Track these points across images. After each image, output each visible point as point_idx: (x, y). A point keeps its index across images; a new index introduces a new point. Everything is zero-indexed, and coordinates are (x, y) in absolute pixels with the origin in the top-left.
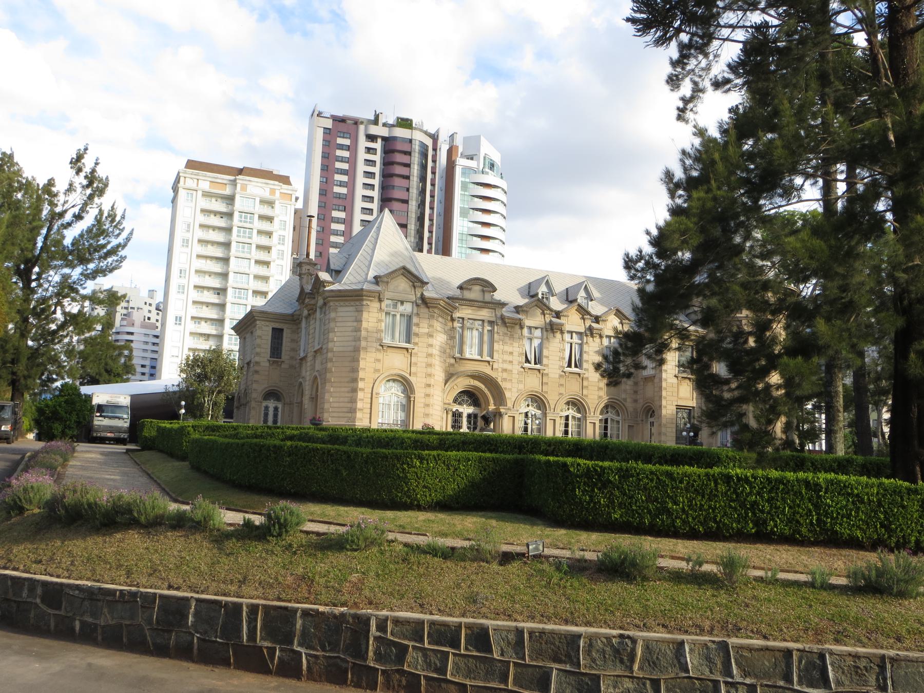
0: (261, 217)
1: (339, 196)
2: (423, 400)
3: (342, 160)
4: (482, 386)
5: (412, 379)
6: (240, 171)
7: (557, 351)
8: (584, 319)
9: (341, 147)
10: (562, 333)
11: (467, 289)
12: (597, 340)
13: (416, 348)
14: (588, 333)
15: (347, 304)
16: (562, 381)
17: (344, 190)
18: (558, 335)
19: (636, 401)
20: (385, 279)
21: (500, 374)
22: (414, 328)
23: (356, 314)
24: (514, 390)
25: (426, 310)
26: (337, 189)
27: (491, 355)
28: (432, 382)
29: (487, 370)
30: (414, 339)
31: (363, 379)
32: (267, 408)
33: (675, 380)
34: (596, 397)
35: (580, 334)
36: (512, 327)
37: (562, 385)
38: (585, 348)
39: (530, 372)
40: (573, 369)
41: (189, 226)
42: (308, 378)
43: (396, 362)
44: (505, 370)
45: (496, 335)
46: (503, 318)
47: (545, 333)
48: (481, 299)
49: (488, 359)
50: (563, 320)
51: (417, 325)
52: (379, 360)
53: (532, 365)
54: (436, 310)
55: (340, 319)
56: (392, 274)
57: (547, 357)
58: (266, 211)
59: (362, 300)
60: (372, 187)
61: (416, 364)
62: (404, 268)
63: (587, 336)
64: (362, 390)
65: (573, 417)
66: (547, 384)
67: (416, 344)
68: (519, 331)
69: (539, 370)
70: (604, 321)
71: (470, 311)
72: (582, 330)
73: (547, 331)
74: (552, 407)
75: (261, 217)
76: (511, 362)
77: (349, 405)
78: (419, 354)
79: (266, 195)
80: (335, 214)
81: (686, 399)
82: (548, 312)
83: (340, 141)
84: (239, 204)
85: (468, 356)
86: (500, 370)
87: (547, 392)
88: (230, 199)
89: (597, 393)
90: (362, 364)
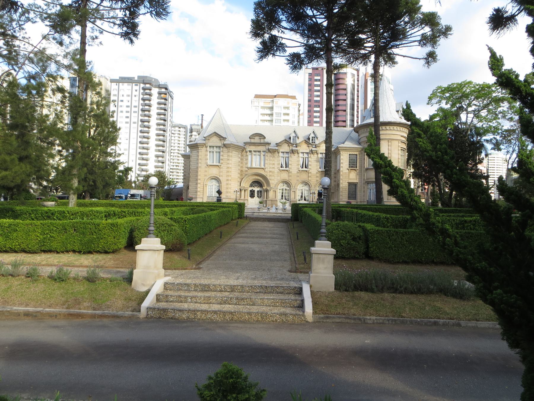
0: (285, 114)
1: (316, 101)
3: (317, 86)
4: (261, 179)
6: (275, 96)
7: (296, 161)
9: (316, 80)
10: (298, 153)
12: (316, 155)
16: (299, 175)
17: (318, 99)
18: (296, 155)
22: (221, 157)
26: (316, 99)
27: (265, 166)
29: (262, 172)
30: (221, 161)
31: (200, 179)
35: (307, 153)
38: (310, 159)
40: (304, 169)
43: (214, 172)
44: (270, 172)
46: (269, 149)
48: (259, 142)
49: (263, 167)
50: (298, 148)
51: (222, 155)
52: (206, 171)
53: (285, 169)
56: (210, 136)
58: (286, 111)
62: (215, 133)
64: (200, 183)
65: (286, 189)
67: (222, 163)
72: (308, 151)
75: (285, 114)
79: (286, 105)
80: (315, 109)
81: (353, 179)
83: (316, 78)
84: (275, 110)
85: (254, 166)
88: (272, 108)
90: (199, 173)
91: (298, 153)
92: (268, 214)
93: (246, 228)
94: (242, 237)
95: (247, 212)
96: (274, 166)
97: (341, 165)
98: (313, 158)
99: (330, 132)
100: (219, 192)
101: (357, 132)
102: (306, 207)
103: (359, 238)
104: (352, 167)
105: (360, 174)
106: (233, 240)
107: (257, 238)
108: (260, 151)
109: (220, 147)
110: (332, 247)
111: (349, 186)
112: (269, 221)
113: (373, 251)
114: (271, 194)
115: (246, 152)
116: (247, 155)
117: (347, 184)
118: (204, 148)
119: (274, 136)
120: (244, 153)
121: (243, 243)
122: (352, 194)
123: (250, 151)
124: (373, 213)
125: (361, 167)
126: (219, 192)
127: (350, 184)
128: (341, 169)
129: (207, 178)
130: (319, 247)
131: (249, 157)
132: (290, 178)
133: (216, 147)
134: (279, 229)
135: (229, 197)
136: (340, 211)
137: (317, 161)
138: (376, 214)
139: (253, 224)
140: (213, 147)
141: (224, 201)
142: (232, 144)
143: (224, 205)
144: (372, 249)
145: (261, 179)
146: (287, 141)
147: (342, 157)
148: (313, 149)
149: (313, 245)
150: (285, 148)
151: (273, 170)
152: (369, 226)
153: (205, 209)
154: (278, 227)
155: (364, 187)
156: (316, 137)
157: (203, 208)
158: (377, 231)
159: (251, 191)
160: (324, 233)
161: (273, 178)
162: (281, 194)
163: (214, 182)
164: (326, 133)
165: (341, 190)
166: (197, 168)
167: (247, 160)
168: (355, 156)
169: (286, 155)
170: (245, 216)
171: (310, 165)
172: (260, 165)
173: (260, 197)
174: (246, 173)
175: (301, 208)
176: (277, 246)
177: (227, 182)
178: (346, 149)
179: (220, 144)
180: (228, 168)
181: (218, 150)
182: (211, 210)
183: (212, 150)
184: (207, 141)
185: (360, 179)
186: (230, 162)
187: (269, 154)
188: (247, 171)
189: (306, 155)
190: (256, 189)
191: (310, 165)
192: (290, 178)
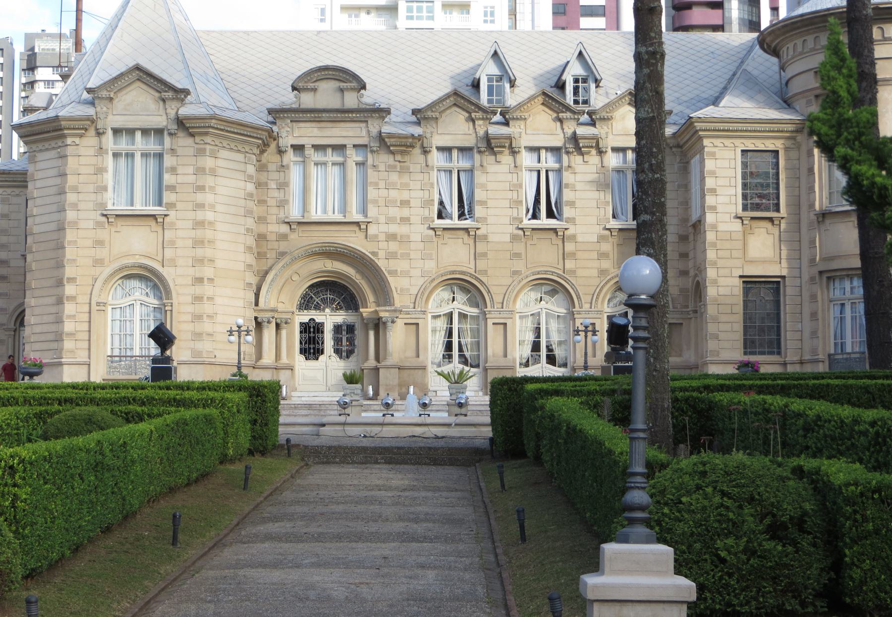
2: (190, 309)
4: (349, 271)
5: (166, 272)
7: (501, 190)
8: (561, 121)
10: (514, 152)
11: (306, 90)
13: (172, 213)
14: (570, 146)
15: (47, 146)
16: (519, 247)
20: (104, 93)
21: (383, 245)
22: (168, 178)
23: (59, 162)
24: (416, 273)
25: (189, 141)
27: (364, 212)
29: (354, 241)
30: (168, 197)
31: (72, 280)
33: (737, 226)
34: (595, 273)
35: (555, 150)
36: (402, 153)
37: (517, 255)
38: (567, 177)
39: (447, 235)
40: (544, 221)
41: (323, 11)
43: (137, 244)
44: (391, 237)
45: (370, 171)
46: (381, 138)
47: (477, 157)
49: (358, 217)
50: (513, 130)
51: (173, 170)
52: (99, 243)
53: (455, 222)
54: (208, 139)
55: (39, 175)
56: (117, 83)
57: (483, 203)
59: (64, 136)
61: (172, 242)
62: (138, 68)
63: (568, 153)
64: (72, 298)
66: (485, 255)
68: (421, 158)
69: (466, 230)
70: (603, 119)
71: (316, 132)
72: (558, 142)
73: (480, 152)
74: (498, 299)
76: (405, 220)
77: (53, 328)
78: (179, 224)
81: (764, 261)
82: (480, 114)
85: (316, 214)
86: (382, 237)
87: (485, 272)
89: (596, 264)
90: (70, 252)
91: (514, 152)
92: (388, 432)
93: (288, 495)
94: (269, 537)
95: (290, 423)
96: (405, 212)
97: (710, 200)
98: (583, 171)
99: (653, 54)
100: (162, 337)
101: (775, 53)
102: (558, 393)
103: (800, 522)
104: (757, 207)
105: (794, 239)
106: (228, 554)
107: (339, 538)
108: (339, 148)
109: (159, 132)
110: (678, 572)
111: (746, 292)
112: (389, 462)
113: (863, 582)
114: (397, 338)
115: (281, 152)
116: (283, 168)
117: (738, 282)
118: (90, 140)
119: (401, 81)
120: (270, 155)
121: (275, 565)
122: (762, 330)
123: (299, 148)
124: (857, 411)
125: (796, 205)
126: (162, 337)
127: (750, 283)
128: (710, 218)
129: (108, 271)
130: (622, 572)
131: (295, 175)
132: (481, 265)
133: (145, 132)
134: (441, 495)
135: (207, 355)
136: (712, 406)
137: (602, 185)
138: (870, 414)
139: (321, 477)
140: (131, 132)
141: (183, 375)
142: (213, 117)
143: (187, 394)
144: (856, 573)
145: (349, 271)
146: (465, 97)
147: (709, 164)
148: (581, 131)
149: (594, 565)
150: (456, 129)
151: (403, 230)
152: (841, 471)
153: (101, 413)
154: (437, 489)
155: (813, 298)
156: (590, 77)
157: (92, 408)
158: (878, 490)
159: (305, 328)
160: (642, 508)
161: (401, 265)
162: (440, 339)
163: (139, 292)
164: (638, 57)
165: (711, 310)
166: (61, 229)
167: (283, 186)
168: (770, 158)
169: (459, 162)
170: (282, 439)
171: (572, 204)
172: (344, 210)
173: (350, 353)
174: (283, 246)
175: (533, 396)
176: (431, 574)
177: (198, 290)
178: (729, 129)
179: (160, 121)
180: (199, 224)
181: (152, 146)
182: (129, 418)
183: (123, 145)
184: (101, 107)
185: (795, 257)
186: (208, 198)
187: (384, 159)
188: (283, 237)
189: (549, 161)
190: (330, 319)
191: (572, 204)
192: (481, 265)
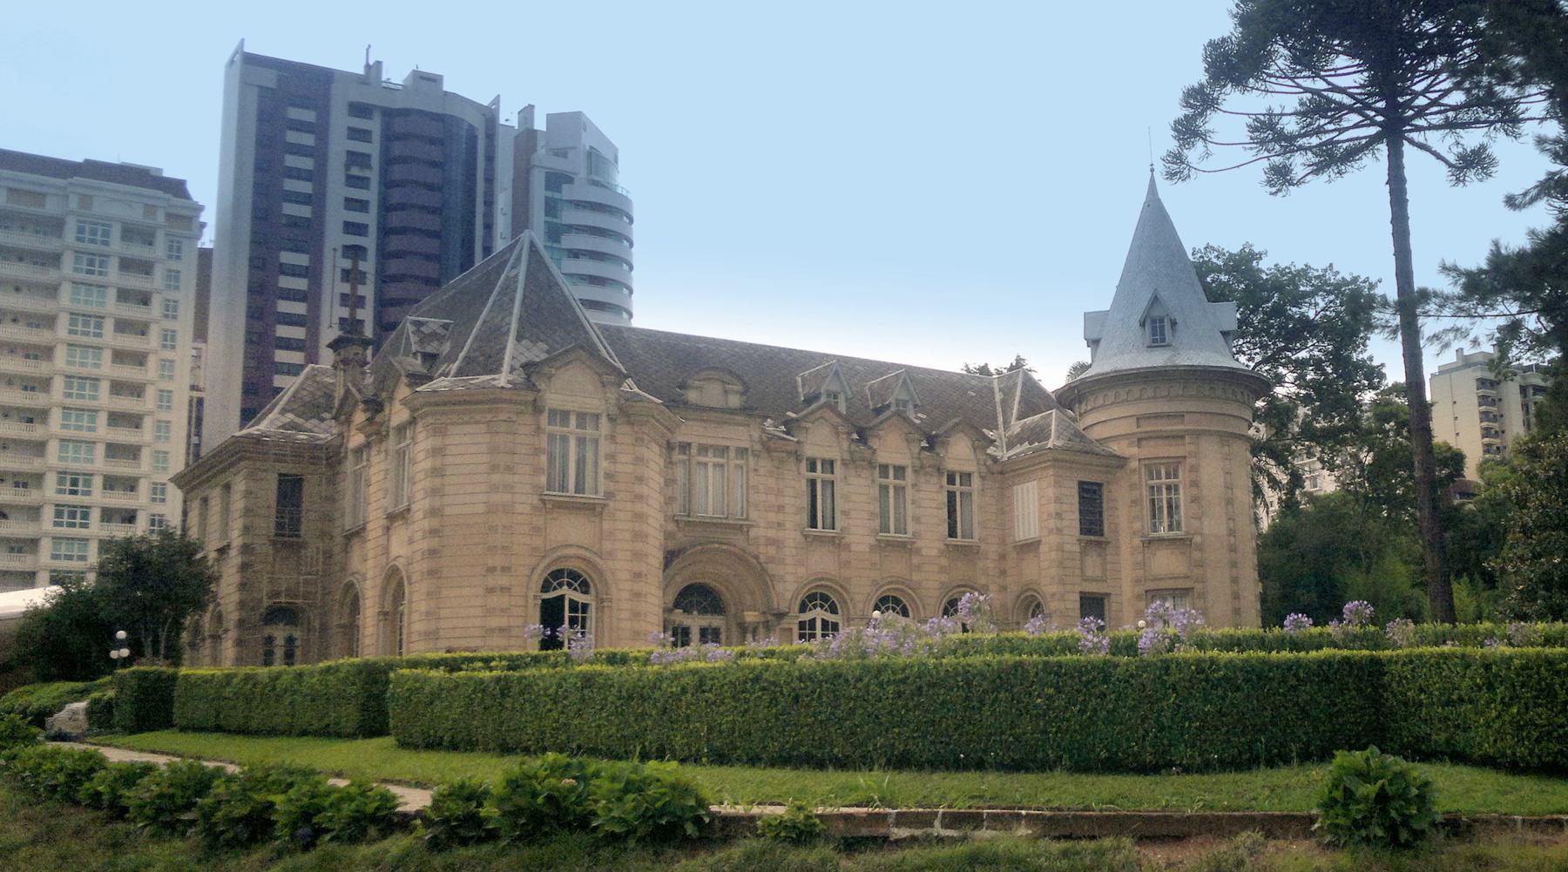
1: (294, 222)
17: (305, 211)
19: (1003, 588)
25: (627, 429)
26: (290, 209)
28: (644, 568)
32: (270, 640)
42: (370, 574)
60: (362, 206)
79: (136, 215)
80: (287, 258)
86: (762, 541)
123: (685, 447)
